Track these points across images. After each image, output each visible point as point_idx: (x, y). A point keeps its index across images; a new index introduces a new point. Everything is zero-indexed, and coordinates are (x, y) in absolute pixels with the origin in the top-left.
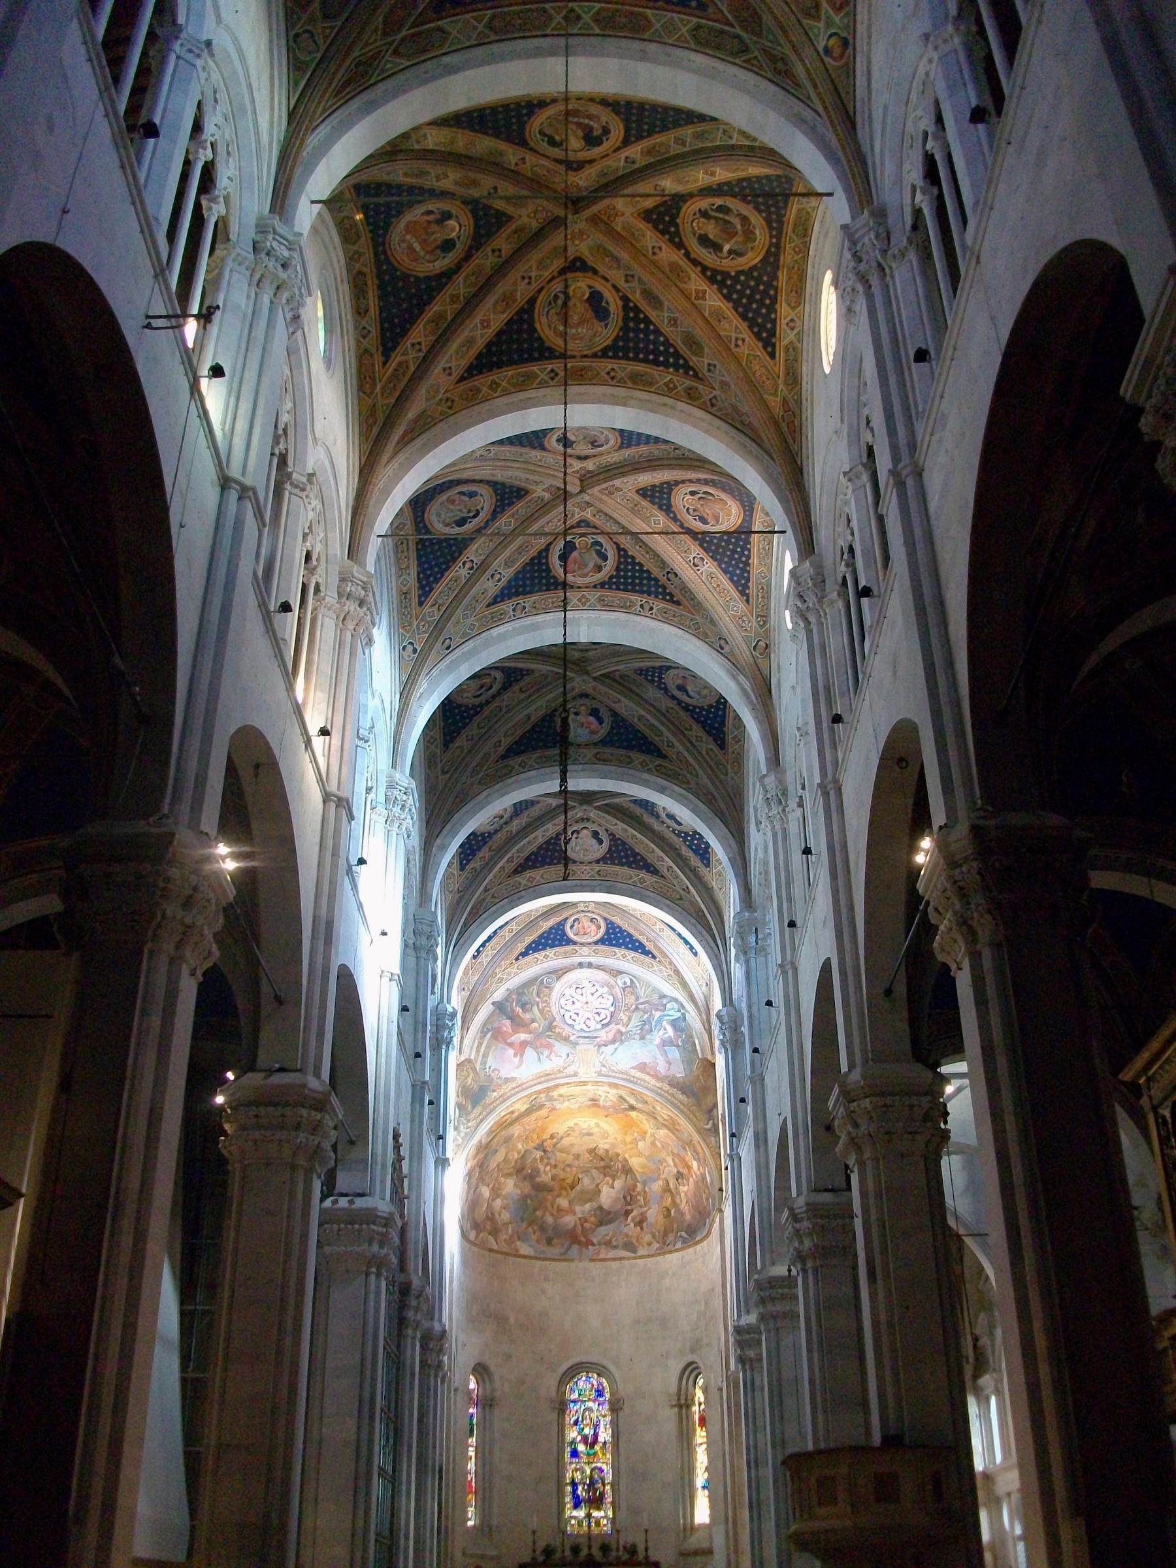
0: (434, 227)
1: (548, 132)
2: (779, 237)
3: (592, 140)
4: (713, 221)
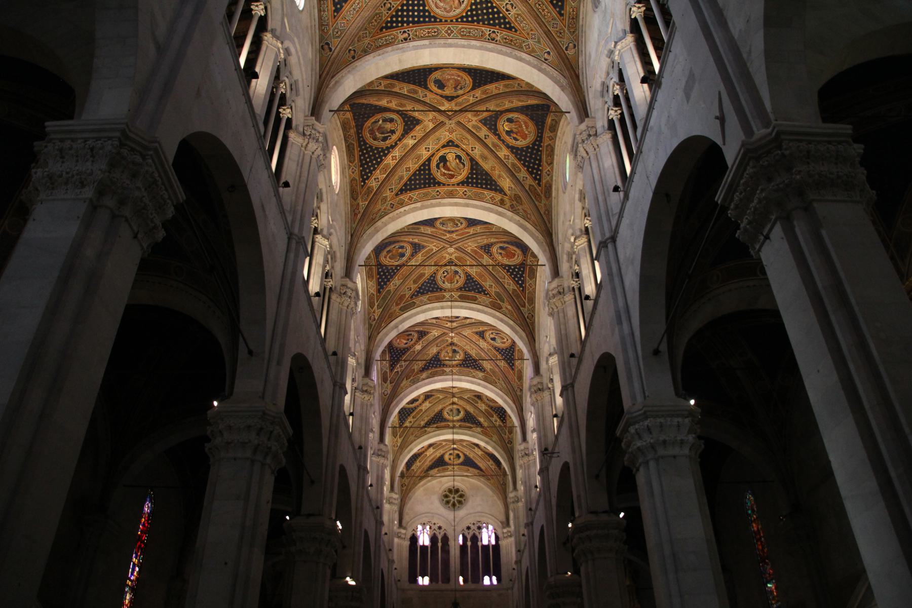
0: (515, 130)
1: (462, 165)
2: (359, 138)
3: (443, 159)
4: (389, 130)
